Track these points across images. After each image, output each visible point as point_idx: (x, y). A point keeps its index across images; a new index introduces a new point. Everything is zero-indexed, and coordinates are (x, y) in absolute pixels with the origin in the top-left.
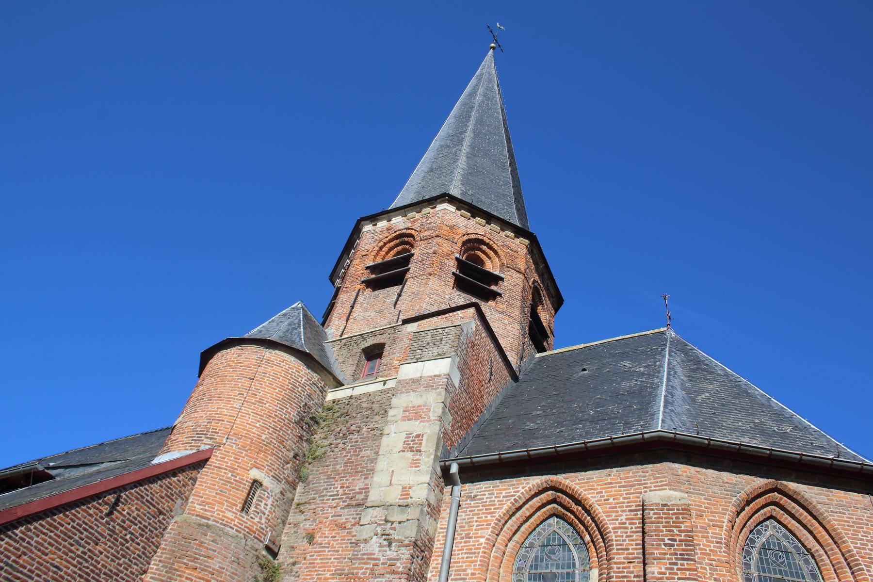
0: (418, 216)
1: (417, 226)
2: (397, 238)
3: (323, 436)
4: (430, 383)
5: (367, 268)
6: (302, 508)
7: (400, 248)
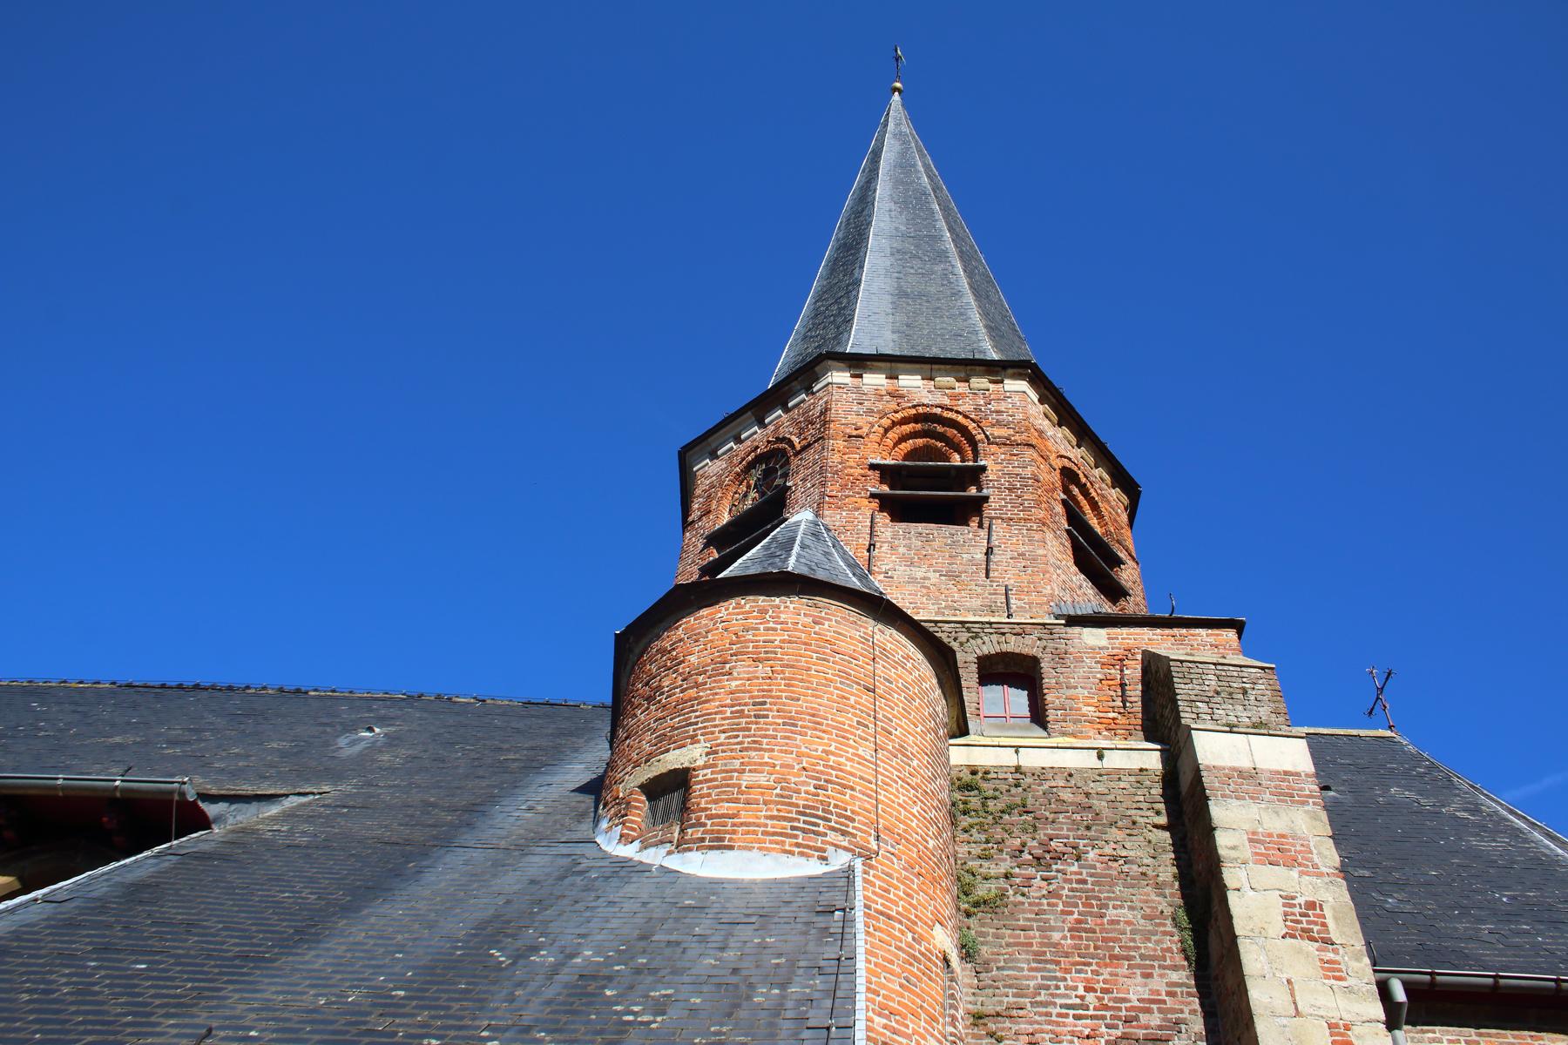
0: (961, 388)
1: (966, 406)
2: (917, 419)
3: (976, 850)
4: (1282, 787)
5: (873, 467)
6: (992, 1026)
7: (920, 442)
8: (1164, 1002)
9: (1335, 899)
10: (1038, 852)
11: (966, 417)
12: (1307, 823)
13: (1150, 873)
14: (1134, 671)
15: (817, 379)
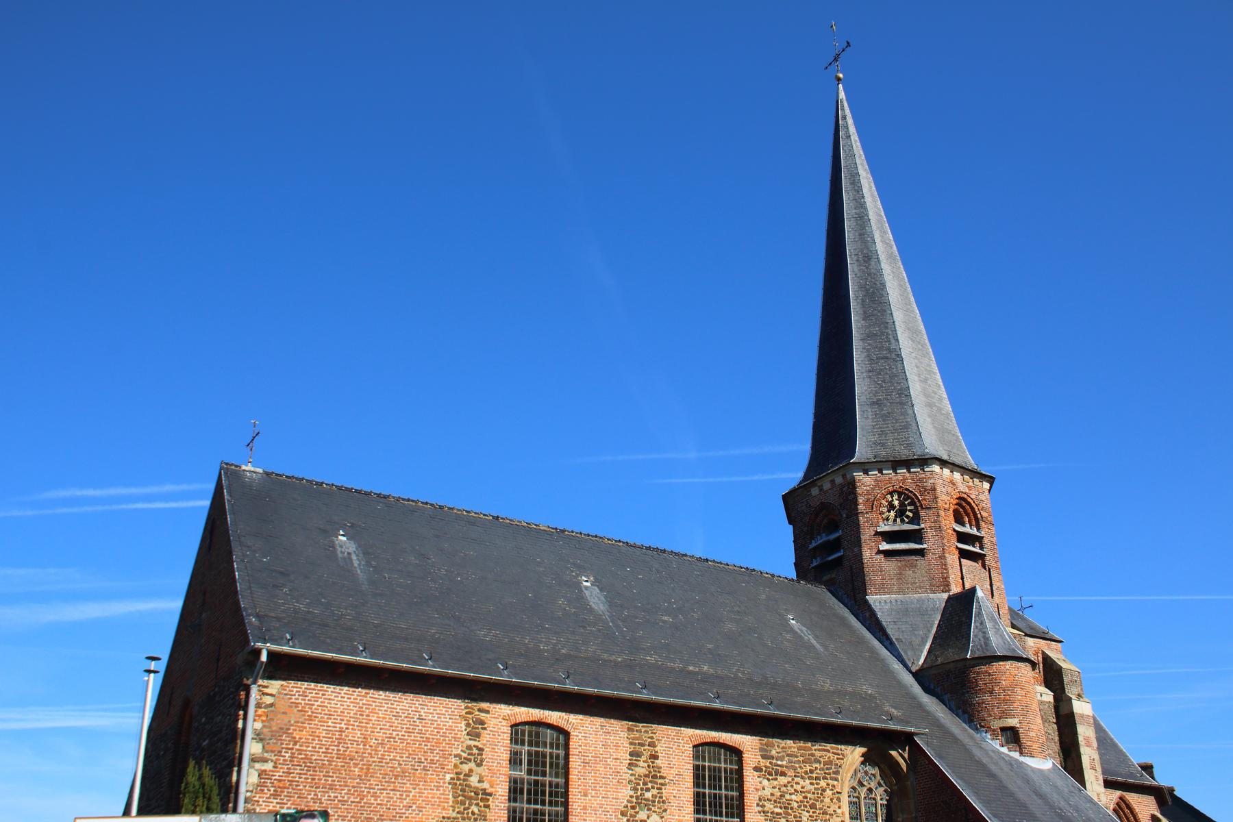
9: (1096, 757)
15: (928, 465)
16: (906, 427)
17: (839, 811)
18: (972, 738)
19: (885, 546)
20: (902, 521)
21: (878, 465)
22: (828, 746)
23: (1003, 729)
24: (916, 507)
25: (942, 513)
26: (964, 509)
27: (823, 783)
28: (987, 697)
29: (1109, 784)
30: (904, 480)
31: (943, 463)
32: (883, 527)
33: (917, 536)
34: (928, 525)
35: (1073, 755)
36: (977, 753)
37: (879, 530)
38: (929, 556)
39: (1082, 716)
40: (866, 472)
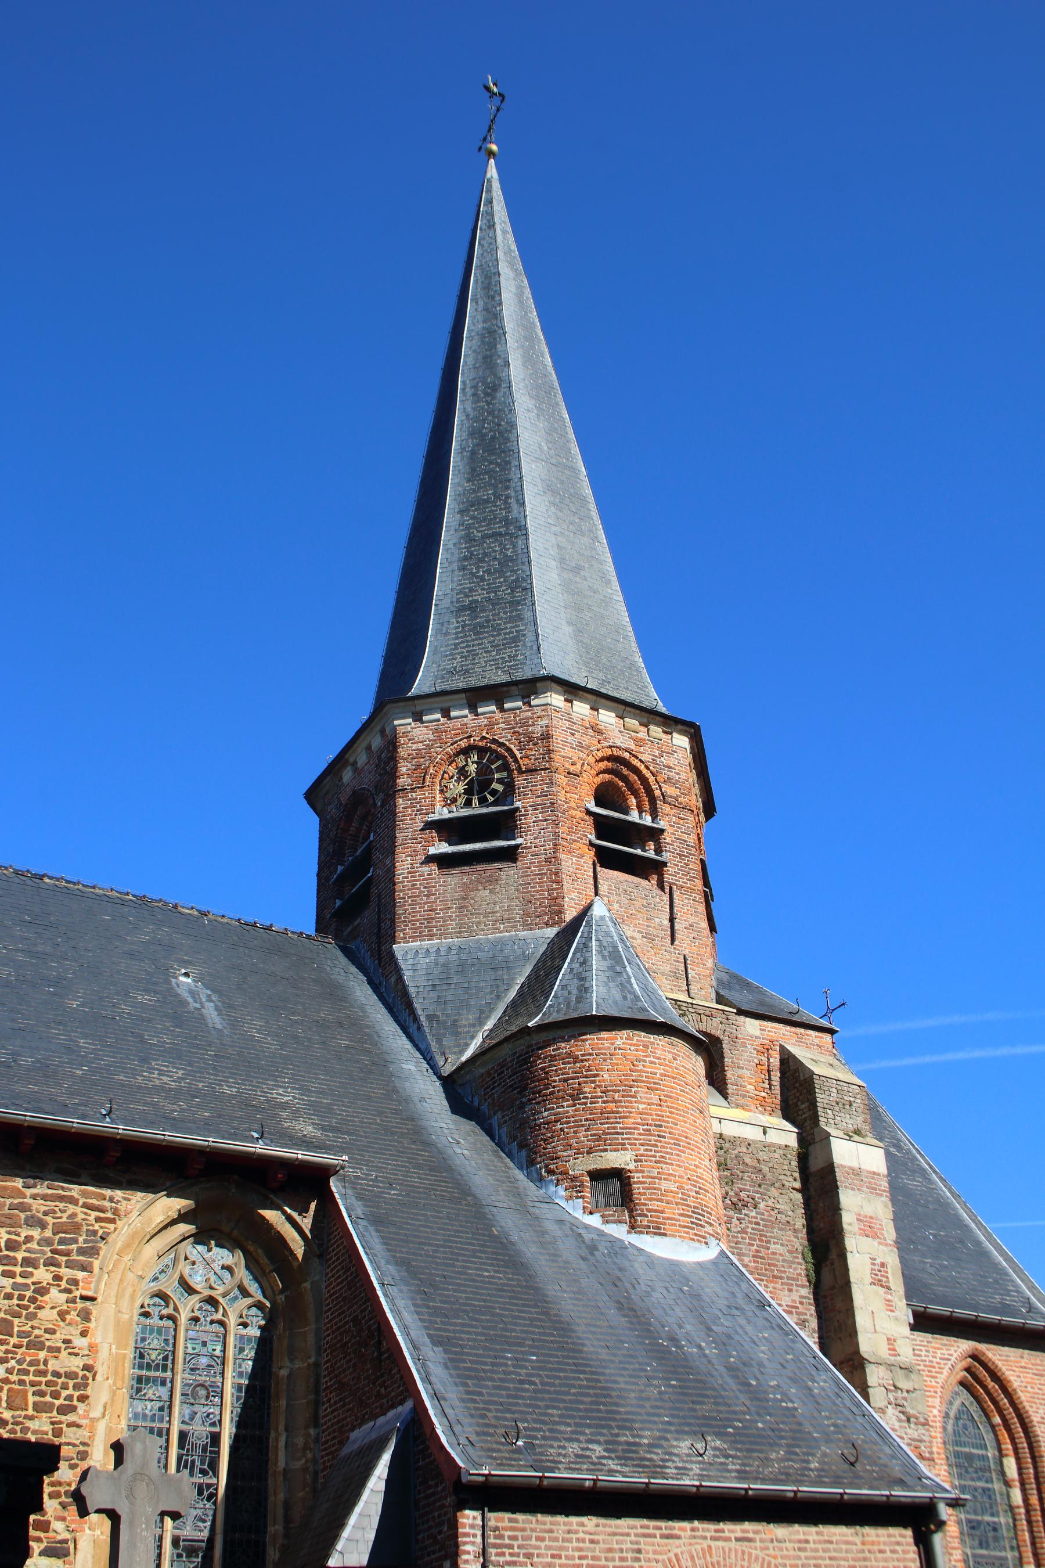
0: (642, 733)
2: (609, 758)
7: (607, 777)
8: (797, 1308)
9: (892, 1259)
10: (734, 1200)
11: (647, 768)
12: (881, 1209)
13: (792, 1222)
14: (775, 1061)
15: (536, 693)
16: (516, 639)
17: (79, 1342)
18: (518, 1195)
19: (445, 848)
20: (483, 801)
21: (442, 700)
22: (75, 1190)
23: (598, 1176)
24: (510, 772)
25: (561, 779)
26: (620, 782)
27: (42, 1275)
28: (566, 1108)
29: (924, 1322)
30: (491, 725)
31: (572, 690)
32: (442, 813)
33: (505, 824)
34: (529, 801)
35: (833, 1255)
36: (508, 1222)
37: (436, 817)
38: (526, 859)
39: (857, 1173)
40: (418, 717)
